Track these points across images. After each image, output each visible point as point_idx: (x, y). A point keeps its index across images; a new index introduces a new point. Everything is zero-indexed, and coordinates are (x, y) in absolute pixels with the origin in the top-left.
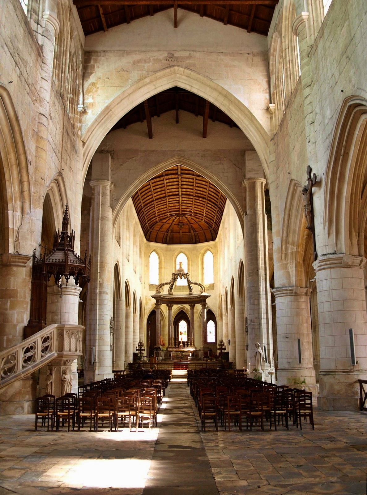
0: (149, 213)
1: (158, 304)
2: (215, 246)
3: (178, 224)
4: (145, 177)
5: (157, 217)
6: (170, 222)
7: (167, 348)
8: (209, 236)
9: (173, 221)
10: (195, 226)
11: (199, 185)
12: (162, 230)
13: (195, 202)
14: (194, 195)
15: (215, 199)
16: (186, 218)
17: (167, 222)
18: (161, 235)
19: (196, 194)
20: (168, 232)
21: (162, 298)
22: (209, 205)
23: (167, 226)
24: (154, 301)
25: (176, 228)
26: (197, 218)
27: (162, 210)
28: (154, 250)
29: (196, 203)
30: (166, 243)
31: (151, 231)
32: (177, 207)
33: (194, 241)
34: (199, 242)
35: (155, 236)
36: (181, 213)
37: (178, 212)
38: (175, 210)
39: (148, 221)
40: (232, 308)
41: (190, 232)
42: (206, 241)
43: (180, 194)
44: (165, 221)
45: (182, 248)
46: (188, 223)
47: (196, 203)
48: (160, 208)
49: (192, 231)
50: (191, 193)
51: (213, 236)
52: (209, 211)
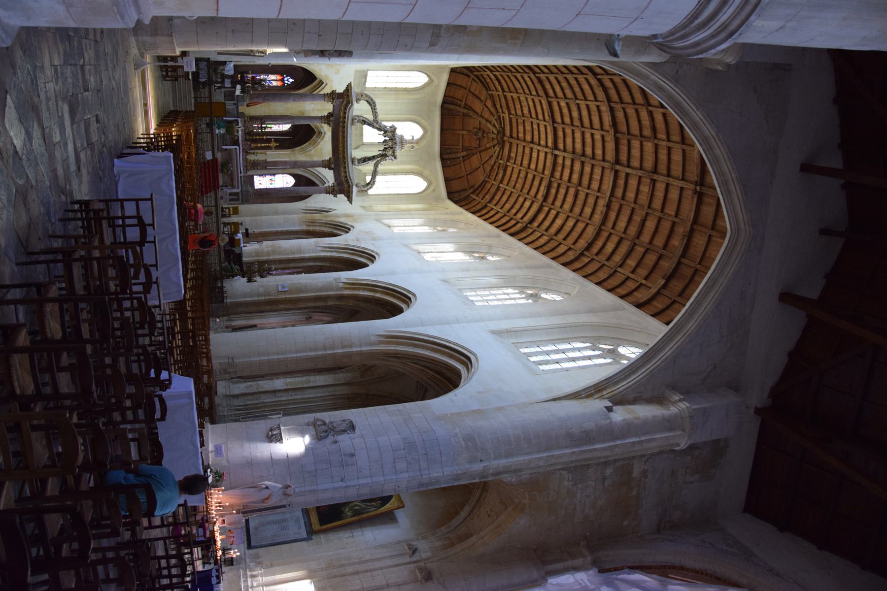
0: (516, 83)
1: (332, 96)
2: (438, 199)
3: (480, 129)
4: (718, 151)
5: (501, 93)
6: (487, 115)
7: (242, 115)
8: (456, 185)
9: (487, 120)
10: (475, 160)
11: (581, 197)
12: (471, 98)
13: (534, 176)
14: (553, 179)
15: (547, 223)
16: (494, 146)
17: (486, 109)
18: (459, 94)
19: (555, 185)
20: (464, 108)
21: (347, 105)
22: (527, 204)
23: (478, 106)
24: (341, 89)
25: (473, 123)
26: (492, 167)
27: (518, 107)
28: (431, 81)
29: (530, 176)
30: (444, 102)
31: (469, 77)
32: (521, 135)
33: (446, 156)
34: (443, 166)
35: (459, 83)
36: (505, 138)
37: (508, 133)
38: (515, 130)
39: (495, 76)
40: (341, 285)
41: (464, 149)
42: (447, 180)
43: (557, 152)
44: (489, 104)
45: (433, 134)
46: (482, 149)
47: (530, 176)
48: (524, 104)
49: (464, 153)
50: (557, 175)
51: (456, 195)
52: (512, 200)
